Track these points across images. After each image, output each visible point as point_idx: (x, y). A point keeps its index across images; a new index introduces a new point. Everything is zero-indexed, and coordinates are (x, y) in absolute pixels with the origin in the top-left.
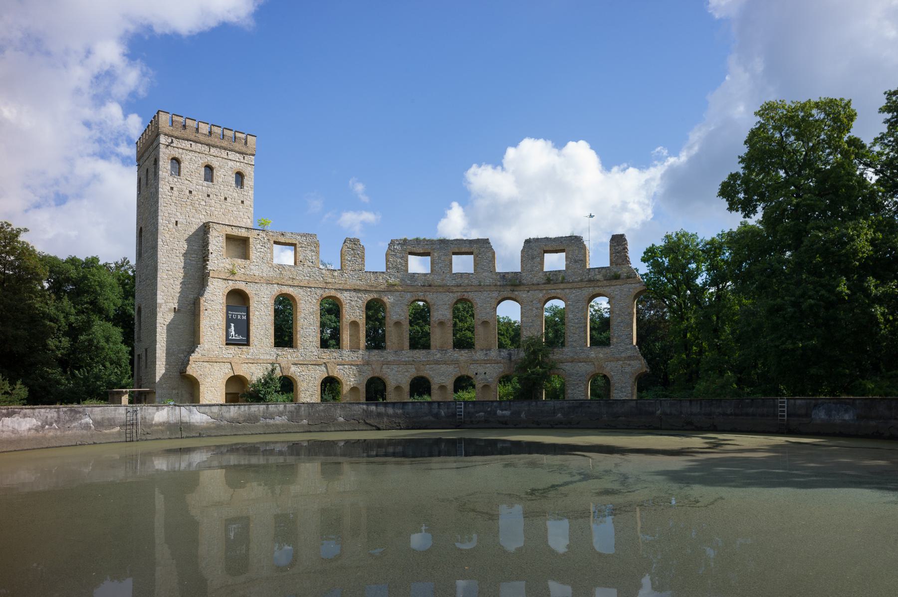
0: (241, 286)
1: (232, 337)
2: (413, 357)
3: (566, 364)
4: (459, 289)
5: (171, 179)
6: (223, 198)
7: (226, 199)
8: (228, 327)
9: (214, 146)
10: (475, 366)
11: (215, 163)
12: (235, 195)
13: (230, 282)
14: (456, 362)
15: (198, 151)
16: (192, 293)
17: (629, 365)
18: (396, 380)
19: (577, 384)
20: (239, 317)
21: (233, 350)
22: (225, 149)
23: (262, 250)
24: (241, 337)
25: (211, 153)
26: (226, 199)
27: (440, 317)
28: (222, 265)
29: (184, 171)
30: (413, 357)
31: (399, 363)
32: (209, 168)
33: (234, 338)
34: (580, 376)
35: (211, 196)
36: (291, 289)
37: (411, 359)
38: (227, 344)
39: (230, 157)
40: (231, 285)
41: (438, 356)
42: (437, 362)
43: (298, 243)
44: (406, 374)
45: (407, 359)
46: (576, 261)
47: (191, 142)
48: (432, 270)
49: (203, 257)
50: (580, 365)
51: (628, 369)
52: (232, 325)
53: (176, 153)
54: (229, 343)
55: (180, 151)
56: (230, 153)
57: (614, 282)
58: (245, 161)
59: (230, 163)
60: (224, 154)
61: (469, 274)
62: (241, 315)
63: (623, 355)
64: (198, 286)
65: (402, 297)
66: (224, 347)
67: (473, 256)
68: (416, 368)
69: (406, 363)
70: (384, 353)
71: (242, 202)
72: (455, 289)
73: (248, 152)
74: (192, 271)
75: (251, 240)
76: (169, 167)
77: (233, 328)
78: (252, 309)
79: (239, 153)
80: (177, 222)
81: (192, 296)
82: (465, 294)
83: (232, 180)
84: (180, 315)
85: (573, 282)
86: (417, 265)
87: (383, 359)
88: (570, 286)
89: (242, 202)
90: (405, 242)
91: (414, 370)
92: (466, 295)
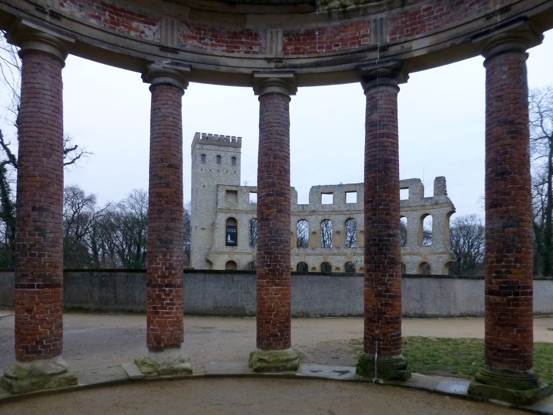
0: (233, 215)
2: (322, 251)
3: (406, 256)
4: (348, 212)
5: (201, 165)
6: (225, 171)
7: (227, 172)
8: (227, 237)
9: (221, 146)
10: (356, 256)
11: (222, 154)
12: (232, 169)
13: (228, 214)
14: (345, 254)
15: (214, 149)
17: (442, 257)
18: (313, 264)
19: (412, 268)
20: (232, 231)
21: (229, 248)
22: (227, 146)
23: (244, 197)
24: (233, 242)
25: (220, 150)
26: (227, 172)
27: (337, 229)
28: (224, 206)
29: (207, 160)
30: (322, 251)
31: (314, 255)
32: (219, 157)
34: (414, 264)
37: (321, 253)
39: (229, 150)
40: (229, 215)
41: (335, 251)
42: (335, 254)
44: (318, 261)
45: (319, 253)
46: (414, 194)
47: (211, 146)
48: (333, 203)
50: (414, 256)
51: (441, 260)
53: (203, 152)
54: (228, 244)
55: (205, 150)
56: (229, 148)
57: (435, 206)
58: (237, 151)
59: (230, 153)
60: (226, 149)
61: (354, 204)
62: (233, 230)
63: (439, 251)
65: (316, 218)
66: (225, 246)
67: (356, 193)
68: (323, 258)
69: (318, 255)
70: (306, 249)
71: (235, 172)
72: (346, 213)
75: (238, 192)
76: (200, 159)
77: (229, 237)
78: (238, 227)
79: (234, 147)
81: (211, 222)
82: (351, 215)
83: (230, 161)
85: (413, 207)
86: (327, 199)
87: (305, 252)
88: (410, 209)
89: (235, 172)
90: (319, 187)
91: (322, 259)
92: (352, 216)
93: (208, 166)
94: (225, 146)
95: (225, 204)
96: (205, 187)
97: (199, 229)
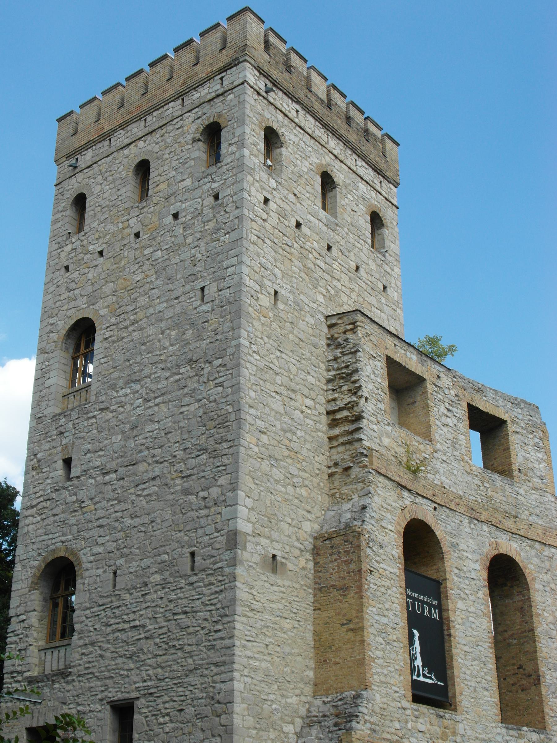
1: (418, 675)
16: (309, 516)
33: (421, 679)
35: (334, 250)
36: (514, 545)
38: (416, 699)
43: (509, 421)
47: (298, 107)
49: (328, 413)
52: (416, 633)
55: (280, 116)
64: (320, 499)
73: (388, 174)
74: (308, 446)
80: (276, 292)
81: (307, 526)
84: (287, 583)
89: (385, 288)
93: (291, 197)
94: (346, 143)
95: (388, 436)
96: (281, 306)
97: (257, 558)
